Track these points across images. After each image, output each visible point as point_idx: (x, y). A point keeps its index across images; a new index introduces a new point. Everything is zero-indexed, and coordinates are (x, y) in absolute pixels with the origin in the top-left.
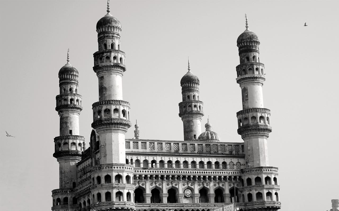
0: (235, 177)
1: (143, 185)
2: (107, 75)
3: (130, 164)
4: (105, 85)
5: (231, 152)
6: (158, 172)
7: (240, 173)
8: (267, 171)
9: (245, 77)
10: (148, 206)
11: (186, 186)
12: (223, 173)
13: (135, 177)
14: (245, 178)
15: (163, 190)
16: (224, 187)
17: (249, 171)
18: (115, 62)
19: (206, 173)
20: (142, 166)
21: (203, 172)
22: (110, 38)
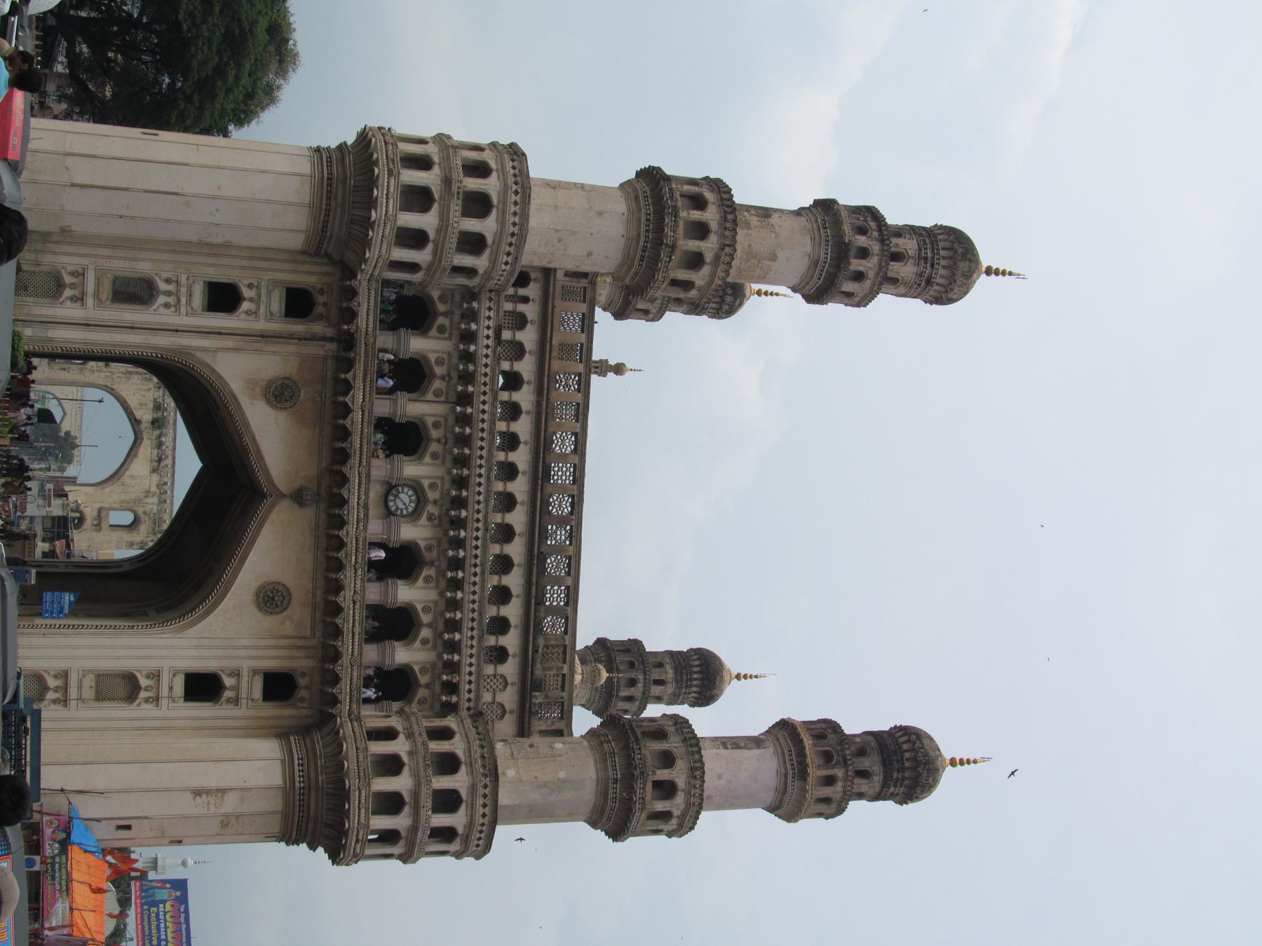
0: (452, 688)
1: (441, 329)
2: (809, 226)
3: (511, 291)
4: (775, 216)
5: (538, 686)
6: (485, 384)
7: (469, 709)
8: (480, 801)
9: (803, 736)
10: (370, 330)
11: (432, 495)
12: (472, 638)
13: (472, 295)
14: (450, 722)
15: (418, 404)
16: (417, 644)
17: (478, 734)
18: (852, 253)
19: (473, 570)
20: (506, 335)
21: (478, 561)
22: (920, 249)
